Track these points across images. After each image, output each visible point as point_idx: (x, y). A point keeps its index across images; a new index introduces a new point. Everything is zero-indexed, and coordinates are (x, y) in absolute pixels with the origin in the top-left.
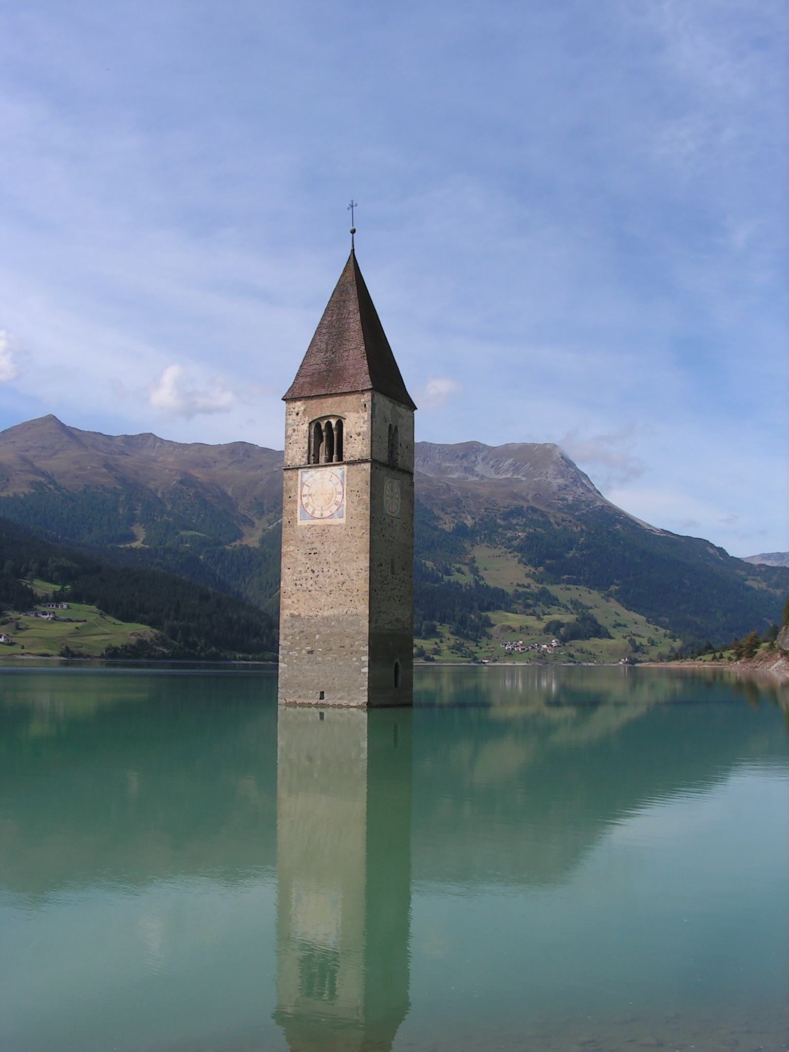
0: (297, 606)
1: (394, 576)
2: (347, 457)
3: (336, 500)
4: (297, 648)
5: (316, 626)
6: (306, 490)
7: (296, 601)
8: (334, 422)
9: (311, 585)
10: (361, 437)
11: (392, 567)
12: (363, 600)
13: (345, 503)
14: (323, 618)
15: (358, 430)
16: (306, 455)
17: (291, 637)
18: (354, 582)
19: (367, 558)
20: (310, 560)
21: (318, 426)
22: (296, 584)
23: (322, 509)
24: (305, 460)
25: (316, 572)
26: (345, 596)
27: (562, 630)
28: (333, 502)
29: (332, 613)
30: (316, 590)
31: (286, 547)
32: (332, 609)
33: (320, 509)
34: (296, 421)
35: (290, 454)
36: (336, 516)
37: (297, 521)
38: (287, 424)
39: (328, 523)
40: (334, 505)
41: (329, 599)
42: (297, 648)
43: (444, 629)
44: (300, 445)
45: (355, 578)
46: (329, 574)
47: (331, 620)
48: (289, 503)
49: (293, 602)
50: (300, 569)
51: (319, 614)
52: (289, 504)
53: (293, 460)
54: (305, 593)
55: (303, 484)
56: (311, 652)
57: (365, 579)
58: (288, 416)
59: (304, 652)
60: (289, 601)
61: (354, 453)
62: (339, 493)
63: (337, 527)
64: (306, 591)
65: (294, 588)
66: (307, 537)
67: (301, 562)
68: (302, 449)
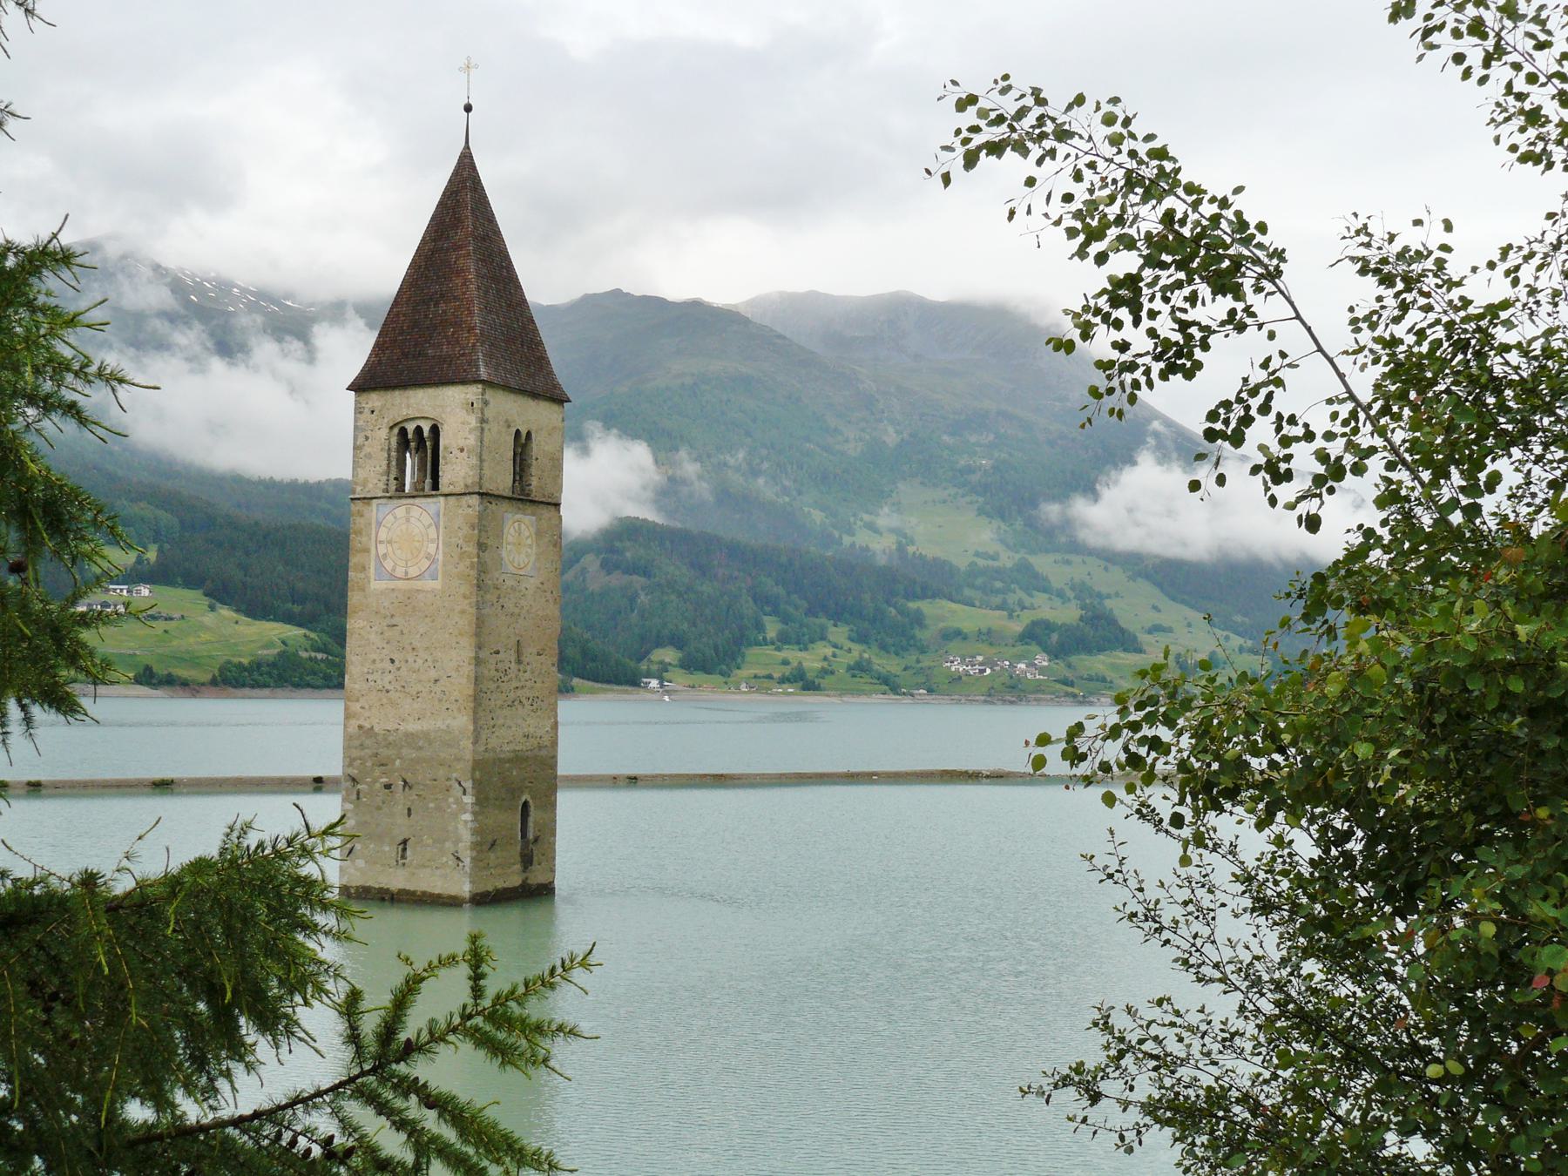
0: (367, 714)
1: (521, 667)
2: (443, 488)
6: (383, 535)
10: (465, 454)
11: (519, 653)
13: (440, 557)
14: (408, 735)
15: (462, 443)
21: (403, 432)
25: (397, 662)
26: (440, 700)
33: (403, 564)
38: (356, 428)
41: (416, 706)
43: (839, 633)
45: (454, 674)
46: (416, 666)
49: (362, 708)
50: (374, 656)
55: (379, 524)
56: (388, 786)
59: (378, 785)
62: (432, 541)
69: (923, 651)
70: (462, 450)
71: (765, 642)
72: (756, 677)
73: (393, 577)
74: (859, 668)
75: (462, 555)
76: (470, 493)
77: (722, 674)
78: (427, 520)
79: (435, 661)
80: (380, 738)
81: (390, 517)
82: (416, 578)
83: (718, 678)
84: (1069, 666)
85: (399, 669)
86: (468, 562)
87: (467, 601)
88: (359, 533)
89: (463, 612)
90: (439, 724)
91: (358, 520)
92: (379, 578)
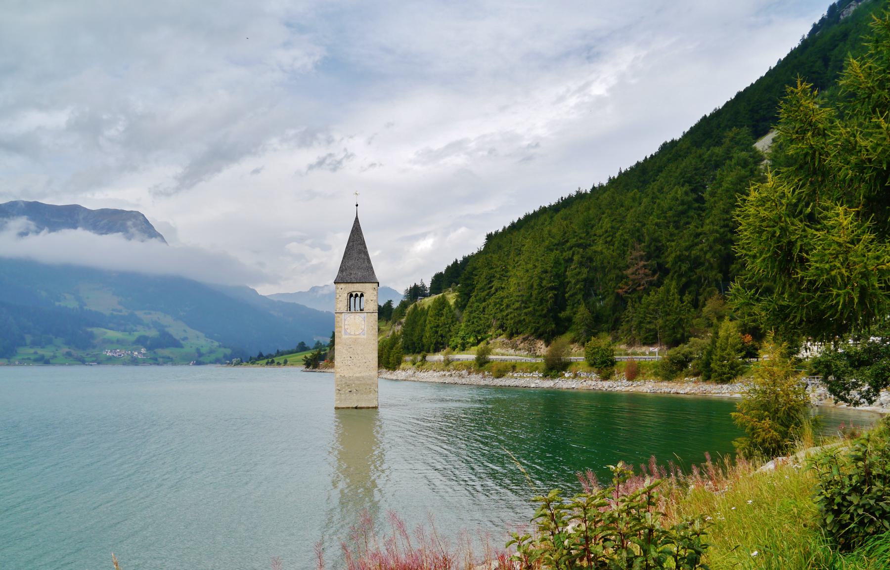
6: (346, 323)
8: (359, 294)
13: (365, 329)
14: (356, 377)
15: (372, 299)
24: (346, 309)
27: (148, 342)
53: (340, 308)
55: (345, 320)
56: (351, 391)
60: (339, 370)
65: (342, 364)
69: (94, 347)
71: (25, 345)
72: (23, 359)
74: (69, 354)
77: (8, 358)
78: (361, 319)
82: (359, 334)
83: (5, 361)
84: (155, 353)
88: (338, 322)
90: (367, 374)
92: (346, 333)
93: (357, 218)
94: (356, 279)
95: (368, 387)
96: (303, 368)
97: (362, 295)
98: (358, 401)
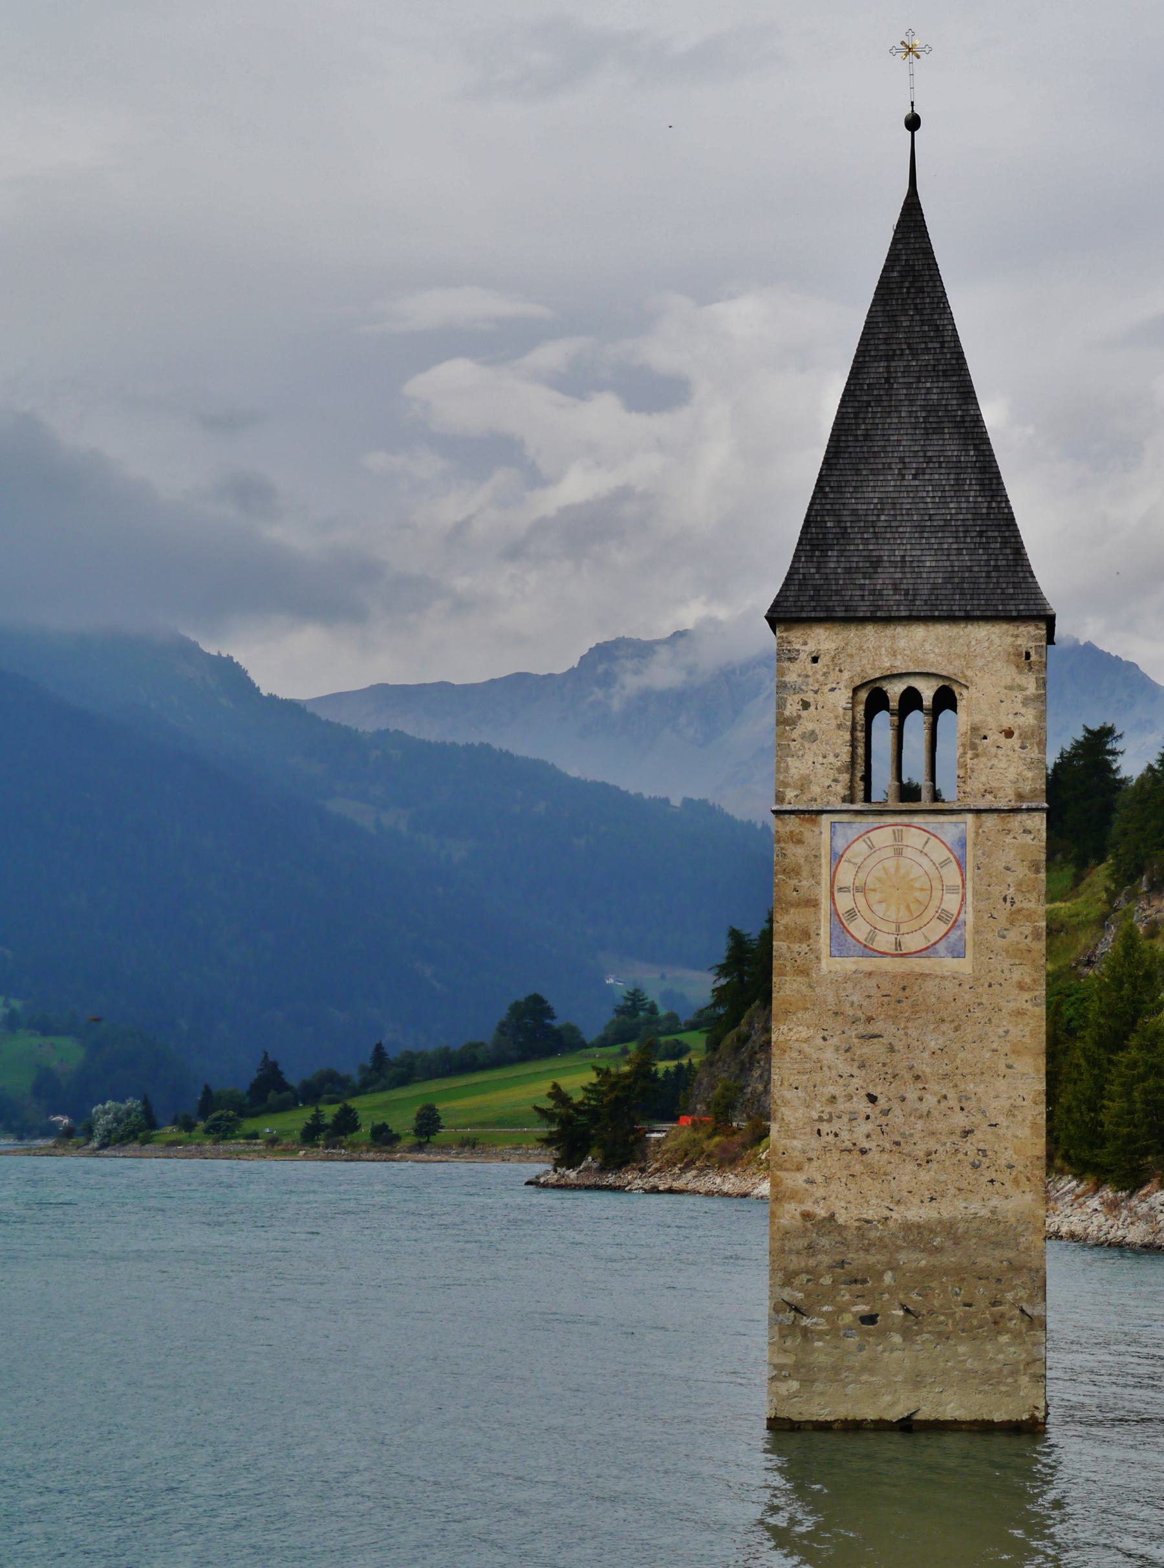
0: (820, 1192)
3: (943, 906)
4: (825, 1308)
5: (886, 1247)
6: (846, 875)
7: (819, 1179)
8: (927, 691)
9: (868, 1136)
10: (1015, 741)
12: (1029, 1180)
13: (969, 917)
14: (908, 1227)
15: (1008, 722)
16: (846, 777)
17: (804, 1277)
18: (1001, 1132)
19: (1038, 1071)
20: (862, 1066)
22: (819, 1132)
23: (898, 929)
24: (841, 789)
25: (882, 1102)
26: (975, 1166)
28: (931, 911)
29: (935, 1215)
30: (883, 1150)
31: (784, 1028)
32: (934, 1203)
33: (893, 926)
34: (810, 680)
35: (793, 771)
36: (942, 952)
37: (818, 958)
38: (782, 686)
39: (917, 970)
40: (935, 922)
41: (925, 1176)
42: (825, 1308)
44: (824, 748)
45: (1002, 1120)
46: (924, 1107)
47: (931, 1231)
48: (792, 905)
49: (810, 1182)
50: (831, 1090)
51: (895, 1215)
52: (792, 911)
53: (804, 784)
54: (845, 1155)
55: (837, 858)
56: (870, 1319)
57: (1034, 1124)
58: (786, 664)
59: (847, 1318)
61: (994, 784)
62: (952, 890)
63: (946, 982)
64: (850, 1151)
65: (815, 1143)
66: (852, 1004)
67: (834, 1072)
68: (831, 758)
70: (1009, 734)
73: (868, 951)
75: (1015, 917)
76: (1029, 810)
79: (963, 1098)
80: (850, 1235)
81: (860, 847)
82: (927, 951)
85: (886, 1113)
86: (1027, 929)
87: (1027, 996)
88: (795, 872)
89: (1020, 1013)
90: (975, 1207)
91: (793, 850)
93: (912, 210)
94: (911, 596)
95: (981, 1292)
96: (540, 1168)
97: (946, 699)
98: (917, 1381)
